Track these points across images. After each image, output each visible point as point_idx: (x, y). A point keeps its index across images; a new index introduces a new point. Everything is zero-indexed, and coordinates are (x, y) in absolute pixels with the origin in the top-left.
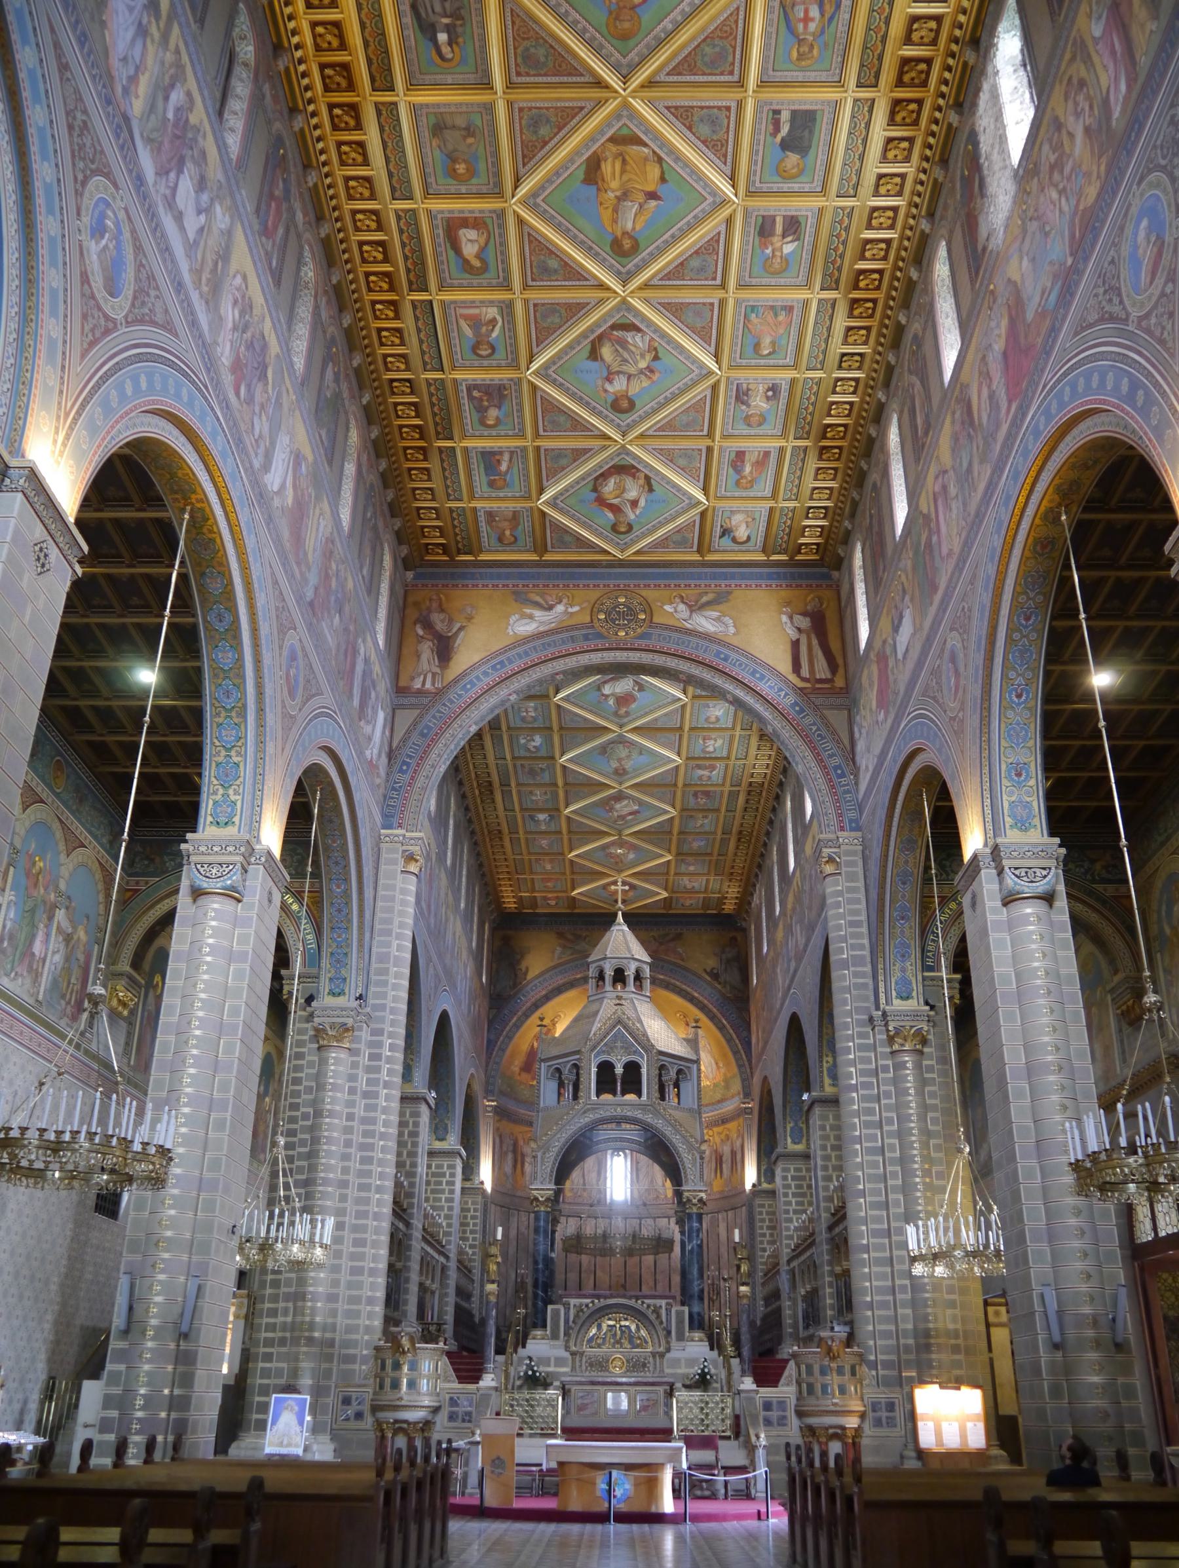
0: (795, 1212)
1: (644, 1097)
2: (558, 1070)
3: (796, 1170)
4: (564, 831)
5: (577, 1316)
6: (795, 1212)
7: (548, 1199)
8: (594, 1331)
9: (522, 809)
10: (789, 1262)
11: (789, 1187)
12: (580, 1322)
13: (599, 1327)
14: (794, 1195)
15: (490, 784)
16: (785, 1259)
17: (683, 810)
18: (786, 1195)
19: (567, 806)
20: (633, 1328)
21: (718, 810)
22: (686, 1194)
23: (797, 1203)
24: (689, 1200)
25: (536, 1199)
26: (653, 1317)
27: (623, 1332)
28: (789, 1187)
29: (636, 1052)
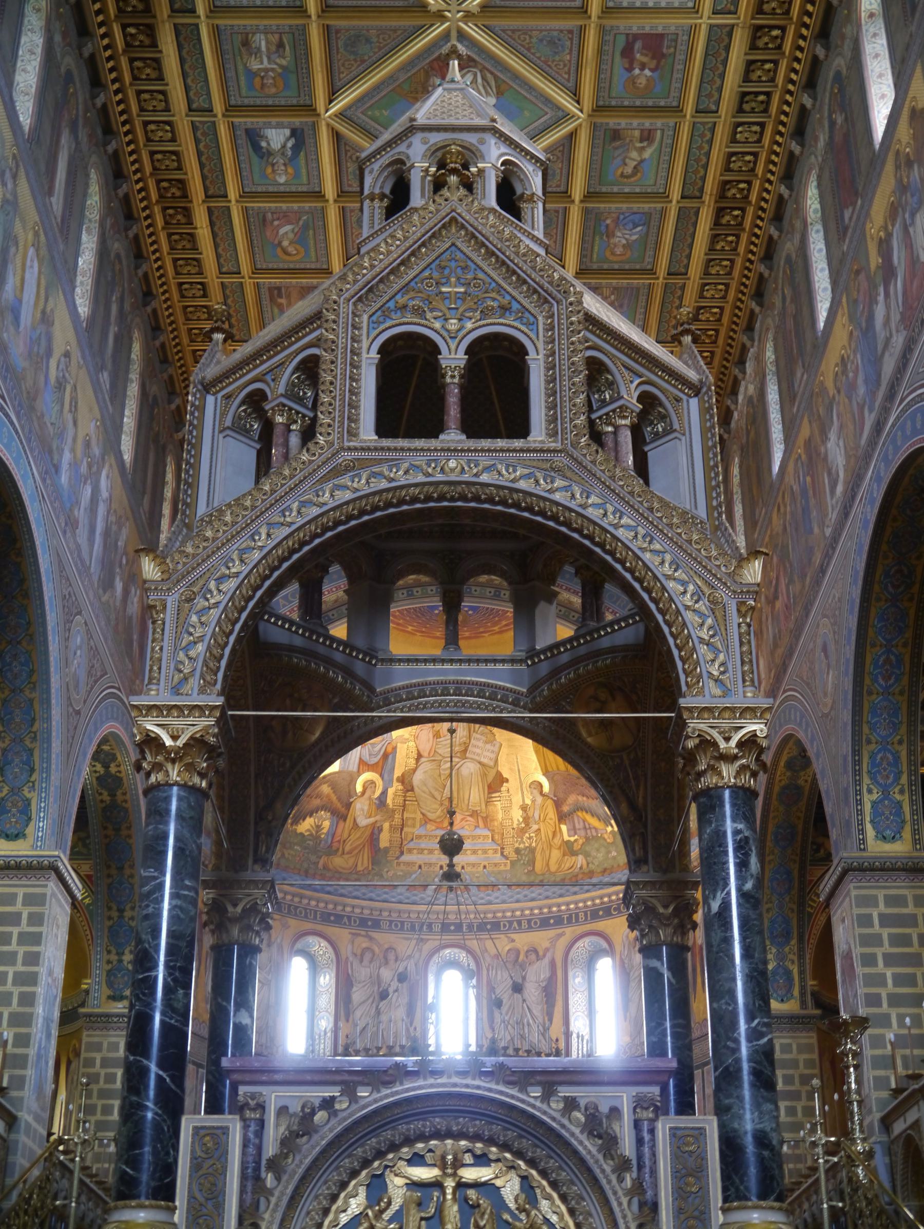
0: (894, 1001)
1: (538, 434)
2: (256, 400)
3: (891, 901)
4: (330, 191)
5: (288, 1144)
6: (894, 1001)
7: (196, 742)
8: (356, 1205)
9: (231, 109)
10: (886, 1123)
11: (876, 940)
12: (297, 1166)
13: (377, 1188)
14: (890, 960)
15: (182, 184)
16: (877, 1116)
17: (598, 109)
18: (869, 960)
19: (332, 95)
20: (510, 1188)
21: (678, 110)
22: (695, 725)
23: (899, 980)
24: (706, 744)
25: (151, 742)
26: (588, 1147)
27: (469, 1208)
28: (876, 940)
29: (505, 309)
